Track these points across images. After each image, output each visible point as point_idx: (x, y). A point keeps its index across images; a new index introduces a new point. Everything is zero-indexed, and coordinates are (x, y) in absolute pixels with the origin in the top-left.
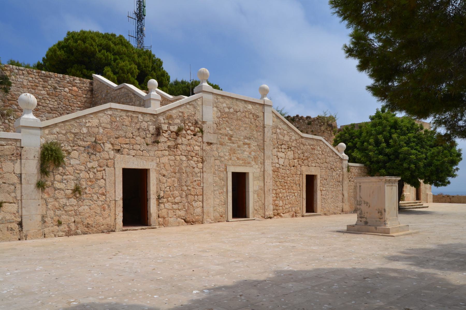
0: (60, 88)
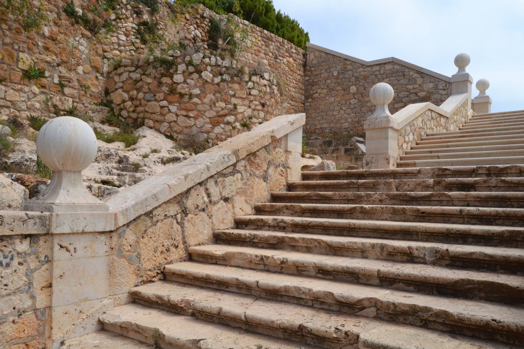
0: (280, 58)
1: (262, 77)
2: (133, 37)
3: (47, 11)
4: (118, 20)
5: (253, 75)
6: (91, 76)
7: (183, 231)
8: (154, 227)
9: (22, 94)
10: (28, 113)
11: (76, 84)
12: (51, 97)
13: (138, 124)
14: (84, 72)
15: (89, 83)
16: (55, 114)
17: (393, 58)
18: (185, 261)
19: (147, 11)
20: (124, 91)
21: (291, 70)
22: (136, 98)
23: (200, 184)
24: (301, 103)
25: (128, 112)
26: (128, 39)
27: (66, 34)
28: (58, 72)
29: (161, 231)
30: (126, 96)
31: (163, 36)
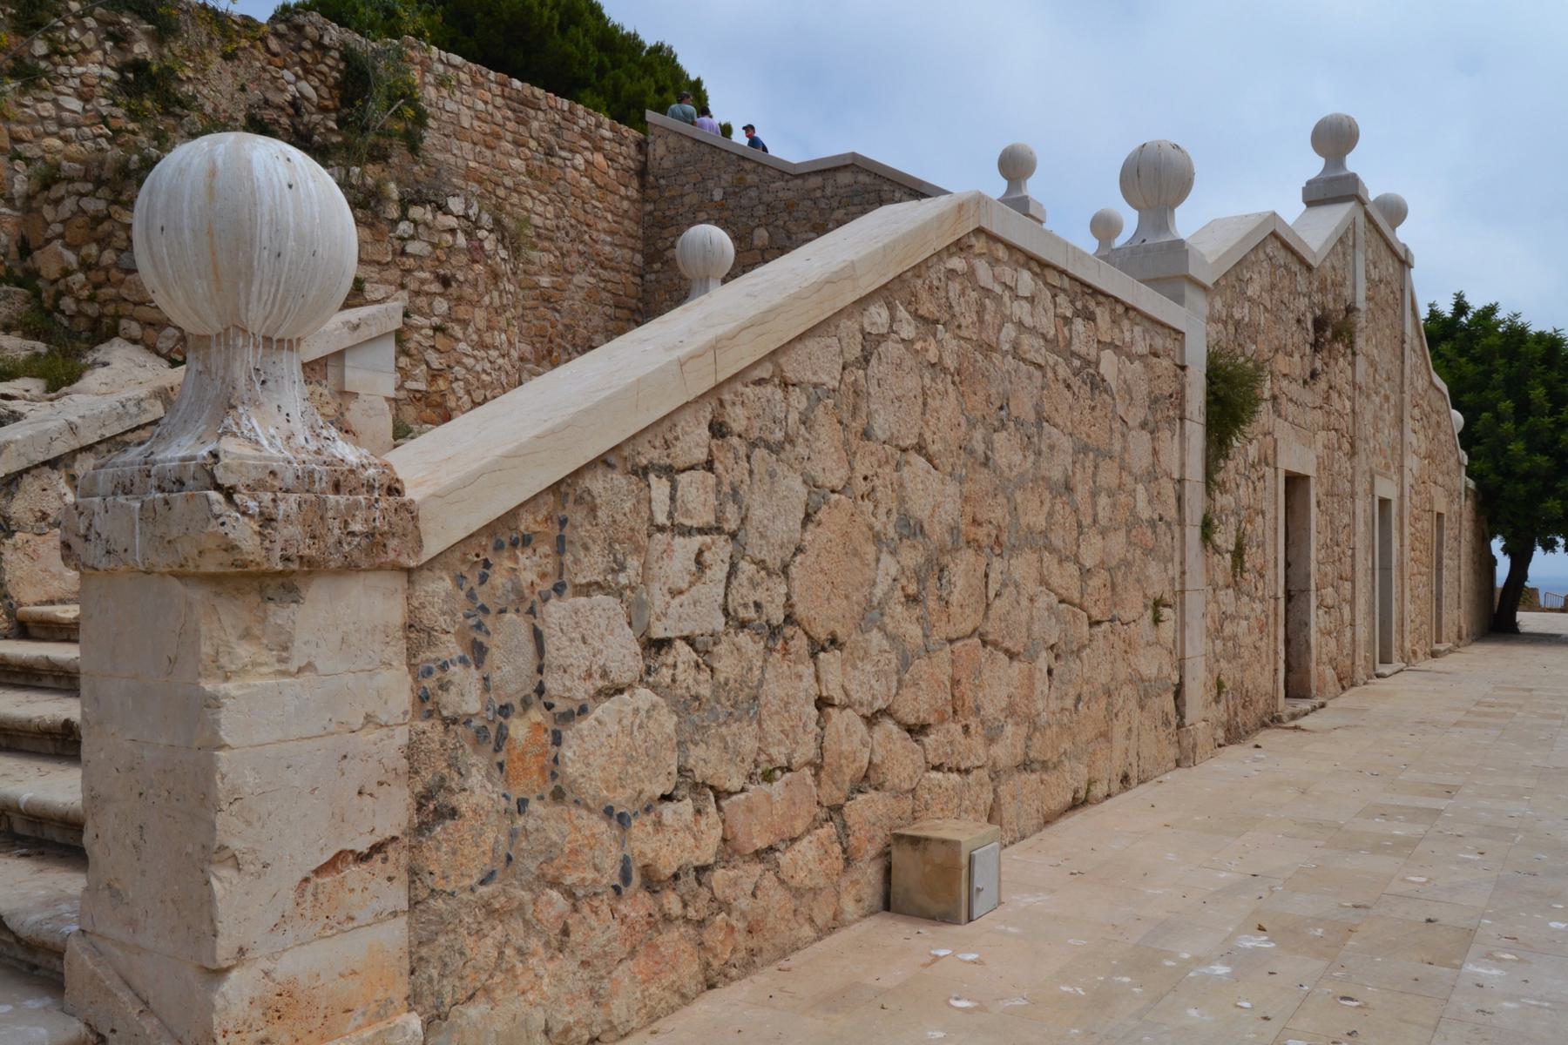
0: (564, 154)
1: (442, 208)
2: (103, 102)
4: (57, 59)
5: (414, 203)
13: (102, 332)
17: (854, 155)
18: (6, 638)
19: (146, 32)
20: (67, 246)
21: (599, 187)
22: (97, 264)
23: (53, 464)
24: (634, 274)
25: (78, 301)
26: (88, 107)
30: (70, 257)
31: (194, 98)
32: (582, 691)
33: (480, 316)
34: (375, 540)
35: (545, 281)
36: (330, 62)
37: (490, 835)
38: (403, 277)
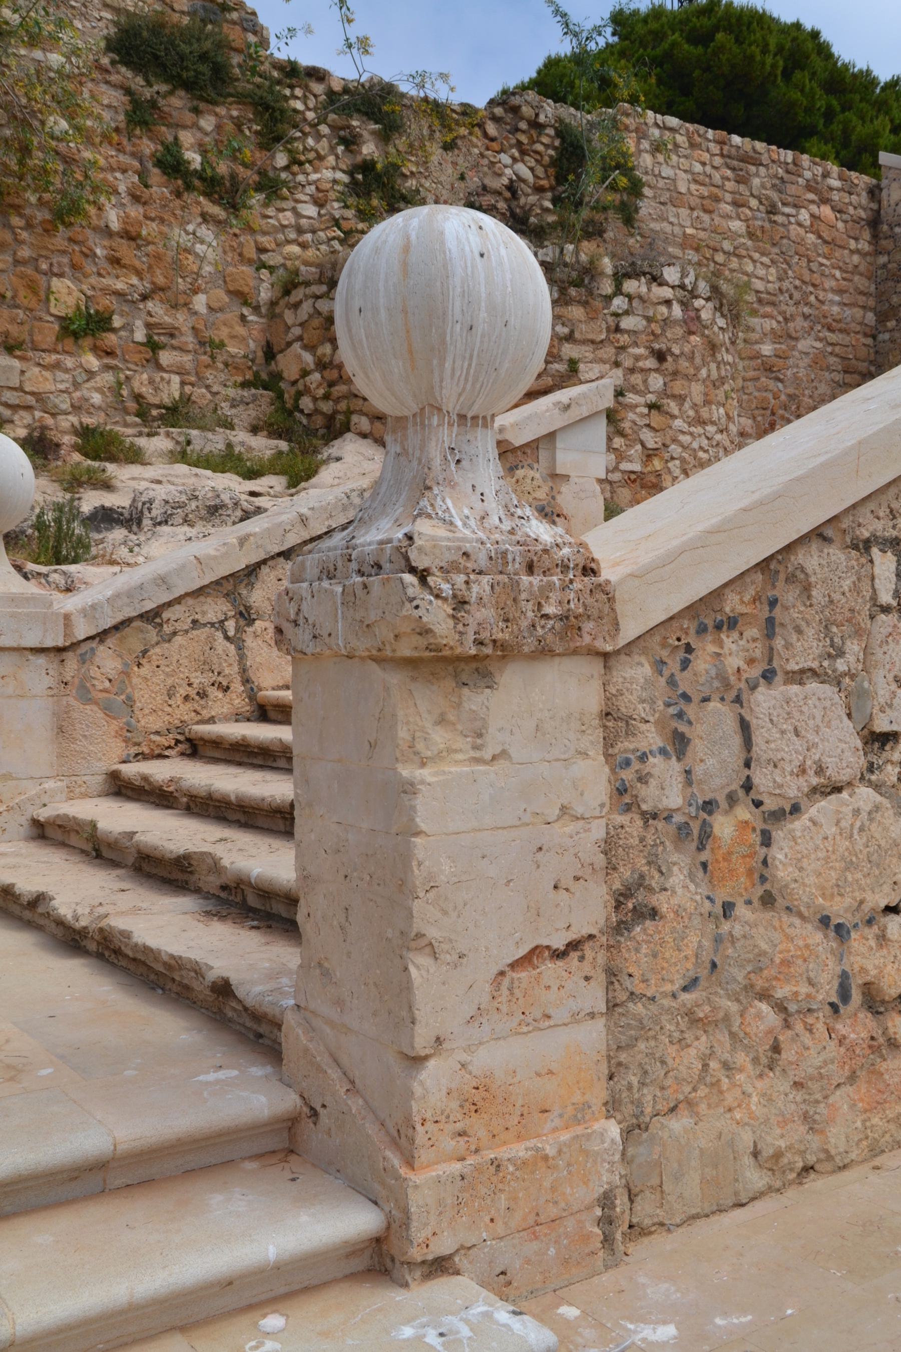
0: (787, 210)
1: (657, 280)
2: (336, 205)
3: (112, 170)
4: (295, 168)
5: (628, 276)
6: (229, 316)
7: (242, 657)
8: (167, 645)
9: (61, 375)
10: (74, 419)
11: (189, 339)
12: (127, 377)
13: (335, 428)
14: (210, 308)
15: (223, 333)
16: (138, 415)
18: (249, 720)
19: (373, 133)
20: (305, 347)
21: (826, 242)
22: (331, 362)
23: (286, 554)
24: (866, 335)
25: (315, 400)
26: (323, 212)
27: (162, 221)
28: (144, 315)
29: (180, 656)
30: (308, 358)
31: (418, 191)
32: (794, 788)
33: (696, 391)
34: (569, 623)
35: (767, 349)
36: (545, 140)
37: (693, 939)
38: (617, 355)
